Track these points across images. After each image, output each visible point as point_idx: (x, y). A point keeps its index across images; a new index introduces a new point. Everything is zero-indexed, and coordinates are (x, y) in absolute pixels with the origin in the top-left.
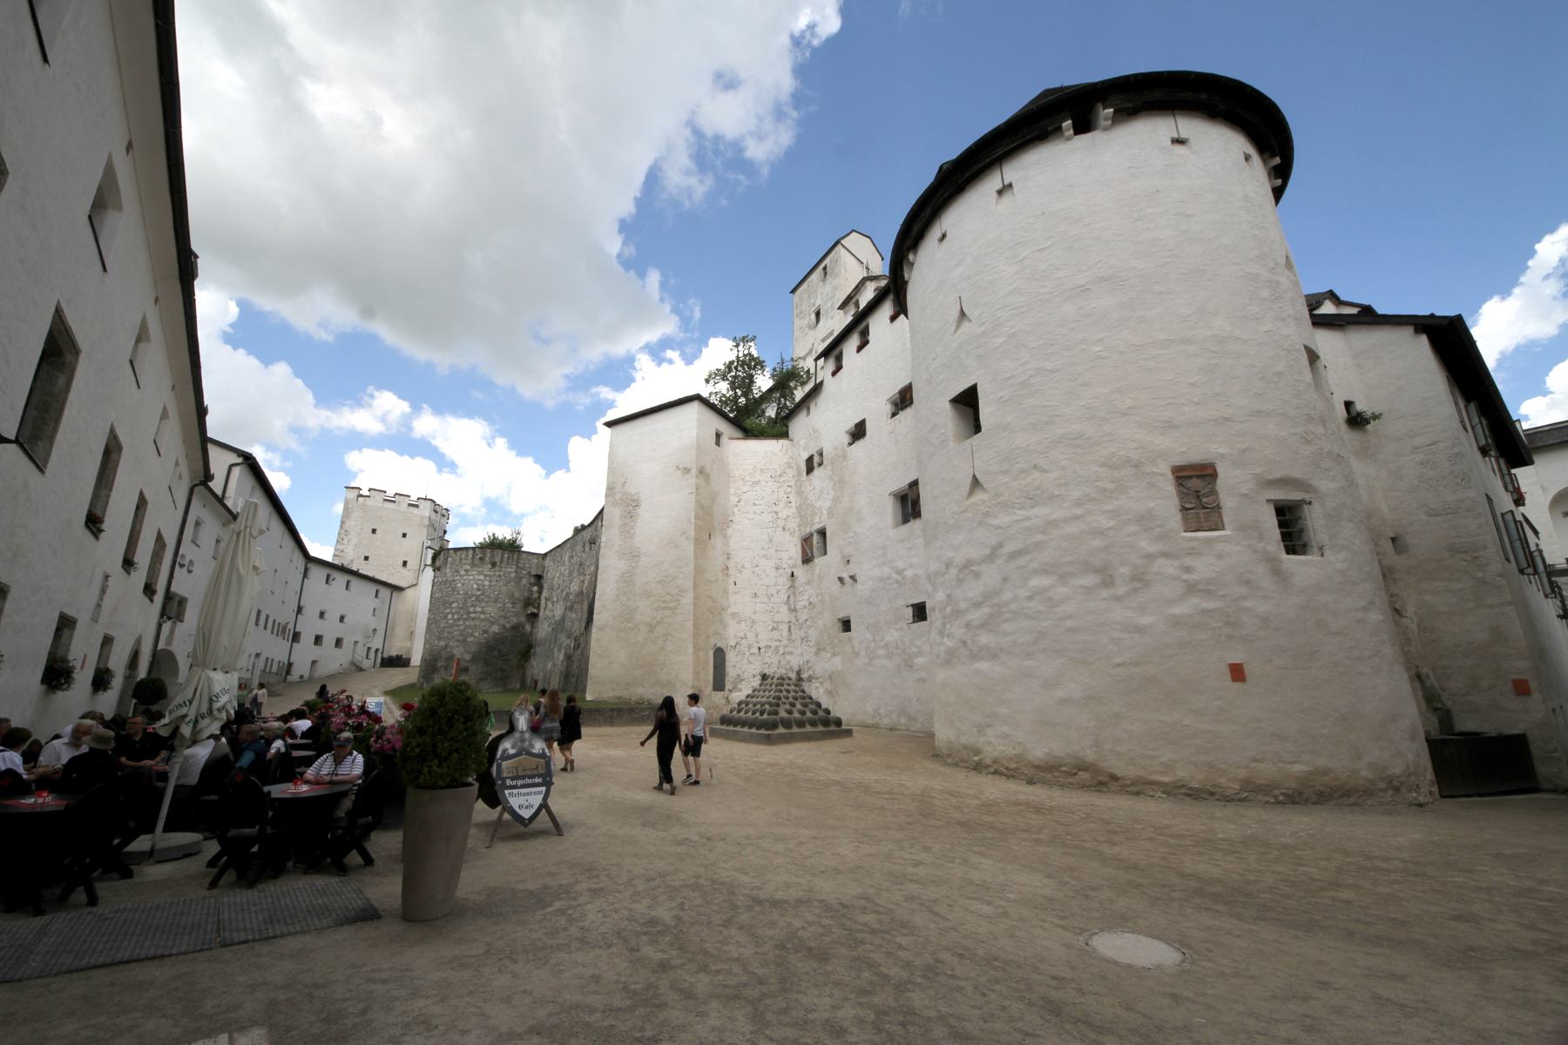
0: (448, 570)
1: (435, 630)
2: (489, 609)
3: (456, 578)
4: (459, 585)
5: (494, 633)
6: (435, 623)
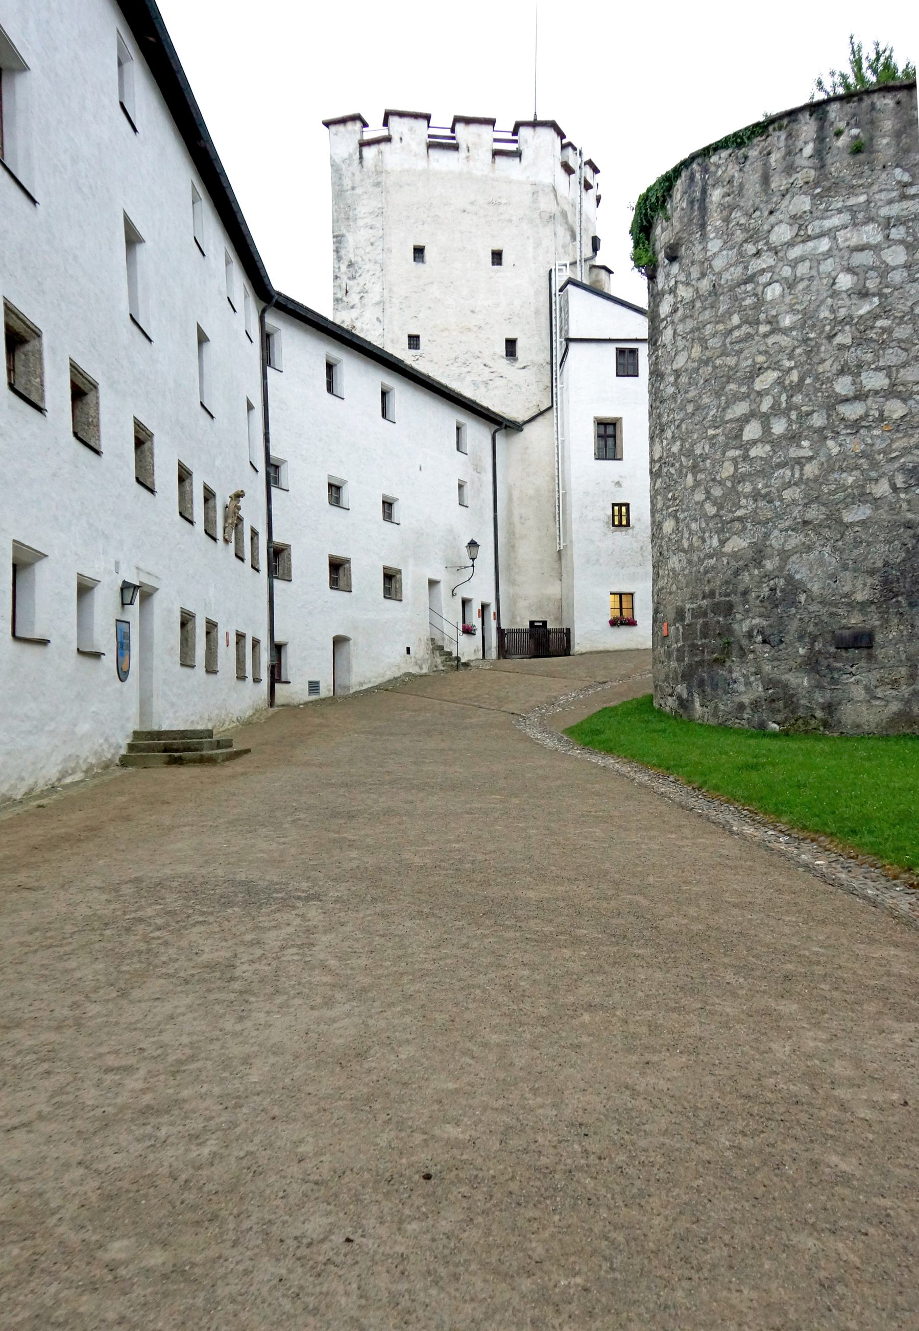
0: (714, 245)
1: (699, 496)
3: (756, 265)
4: (774, 292)
6: (695, 469)
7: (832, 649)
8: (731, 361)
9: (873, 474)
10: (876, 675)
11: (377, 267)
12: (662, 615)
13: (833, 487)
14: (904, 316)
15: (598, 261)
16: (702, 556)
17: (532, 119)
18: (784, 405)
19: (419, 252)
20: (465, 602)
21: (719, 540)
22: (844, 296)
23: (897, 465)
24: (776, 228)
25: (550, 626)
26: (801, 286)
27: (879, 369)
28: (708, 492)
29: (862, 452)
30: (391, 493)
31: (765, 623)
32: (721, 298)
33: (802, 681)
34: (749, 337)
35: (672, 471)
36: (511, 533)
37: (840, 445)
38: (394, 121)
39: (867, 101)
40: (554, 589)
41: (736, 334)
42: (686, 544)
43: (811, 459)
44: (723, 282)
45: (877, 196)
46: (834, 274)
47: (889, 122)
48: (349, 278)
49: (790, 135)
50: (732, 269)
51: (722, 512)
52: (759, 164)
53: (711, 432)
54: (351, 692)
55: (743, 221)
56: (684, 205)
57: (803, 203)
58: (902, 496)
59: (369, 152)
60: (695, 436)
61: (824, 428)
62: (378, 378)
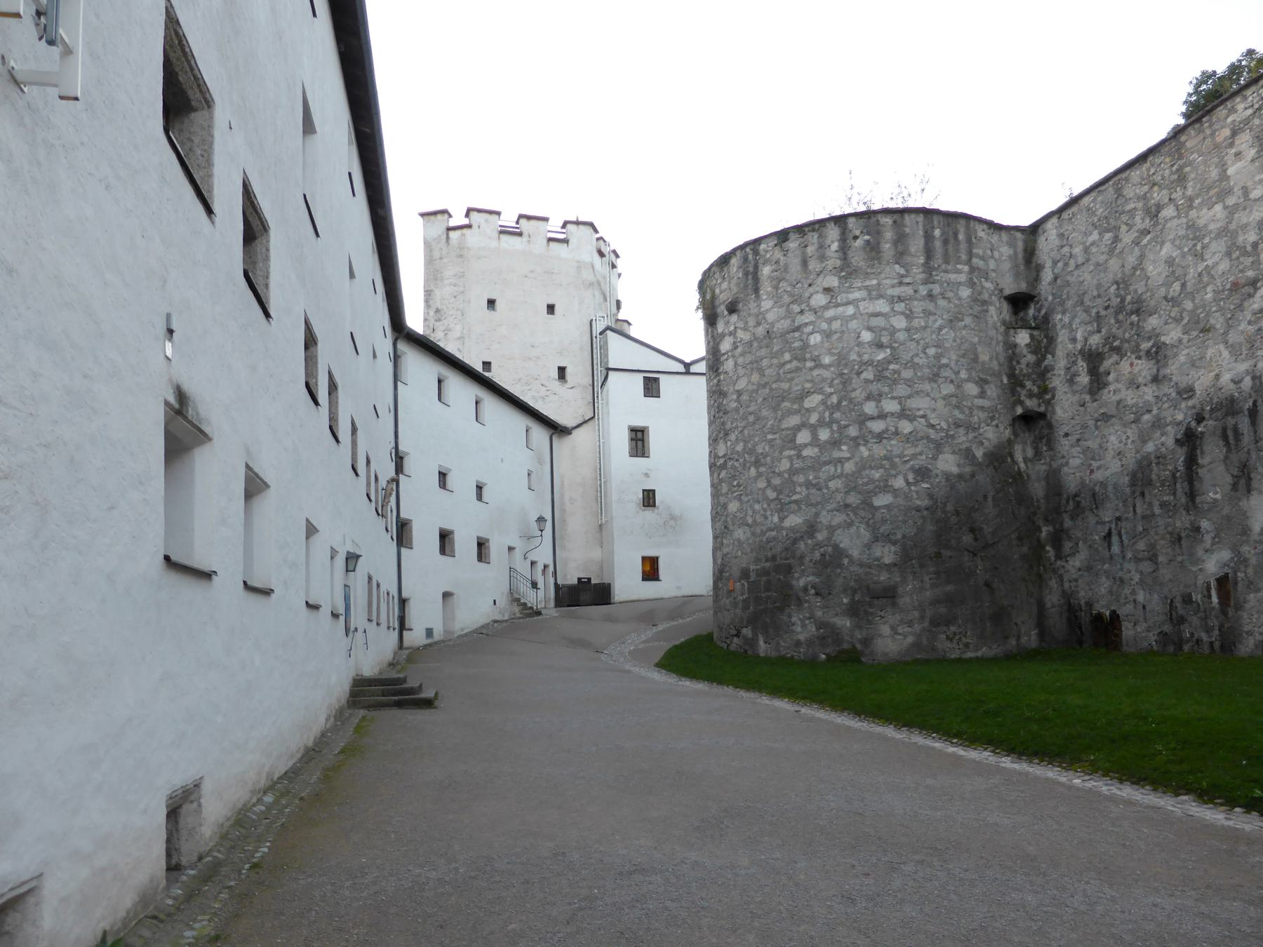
0: (767, 304)
1: (761, 484)
2: (920, 404)
4: (815, 339)
5: (948, 476)
6: (757, 463)
7: (868, 599)
8: (785, 386)
9: (893, 472)
10: (898, 617)
11: (459, 313)
12: (727, 574)
13: (866, 480)
14: (907, 364)
15: (621, 316)
16: (764, 529)
17: (575, 219)
18: (827, 420)
19: (491, 303)
20: (533, 563)
21: (779, 518)
22: (867, 346)
23: (908, 466)
24: (814, 296)
25: (593, 582)
26: (835, 337)
27: (893, 398)
28: (769, 481)
29: (885, 456)
30: (483, 480)
31: (817, 580)
32: (775, 341)
33: (845, 623)
34: (798, 369)
35: (737, 464)
36: (564, 511)
37: (869, 450)
38: (474, 215)
39: (873, 219)
40: (597, 554)
41: (788, 366)
42: (750, 520)
43: (848, 459)
44: (775, 329)
45: (884, 281)
46: (858, 330)
47: (889, 234)
48: (436, 321)
49: (820, 236)
50: (782, 321)
51: (781, 497)
52: (798, 252)
53: (770, 437)
54: (456, 636)
55: (789, 289)
56: (740, 275)
57: (833, 281)
58: (913, 488)
59: (453, 234)
60: (757, 439)
61: (857, 437)
62: (473, 391)
